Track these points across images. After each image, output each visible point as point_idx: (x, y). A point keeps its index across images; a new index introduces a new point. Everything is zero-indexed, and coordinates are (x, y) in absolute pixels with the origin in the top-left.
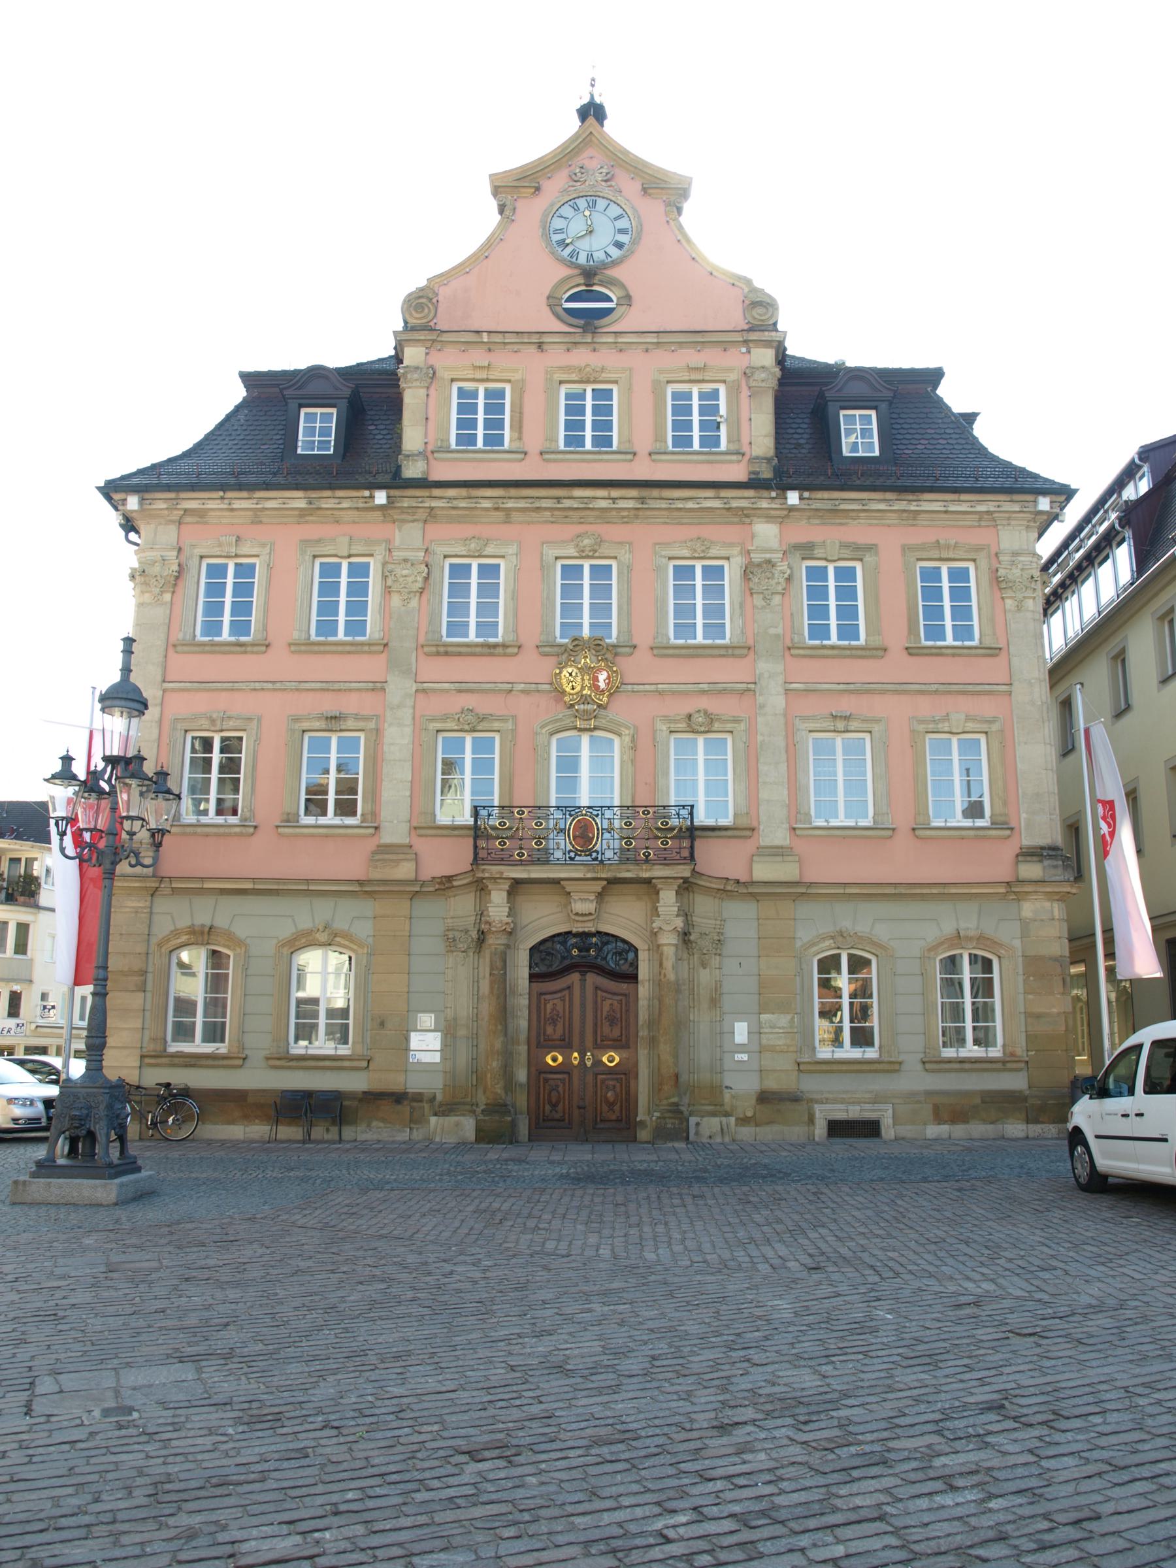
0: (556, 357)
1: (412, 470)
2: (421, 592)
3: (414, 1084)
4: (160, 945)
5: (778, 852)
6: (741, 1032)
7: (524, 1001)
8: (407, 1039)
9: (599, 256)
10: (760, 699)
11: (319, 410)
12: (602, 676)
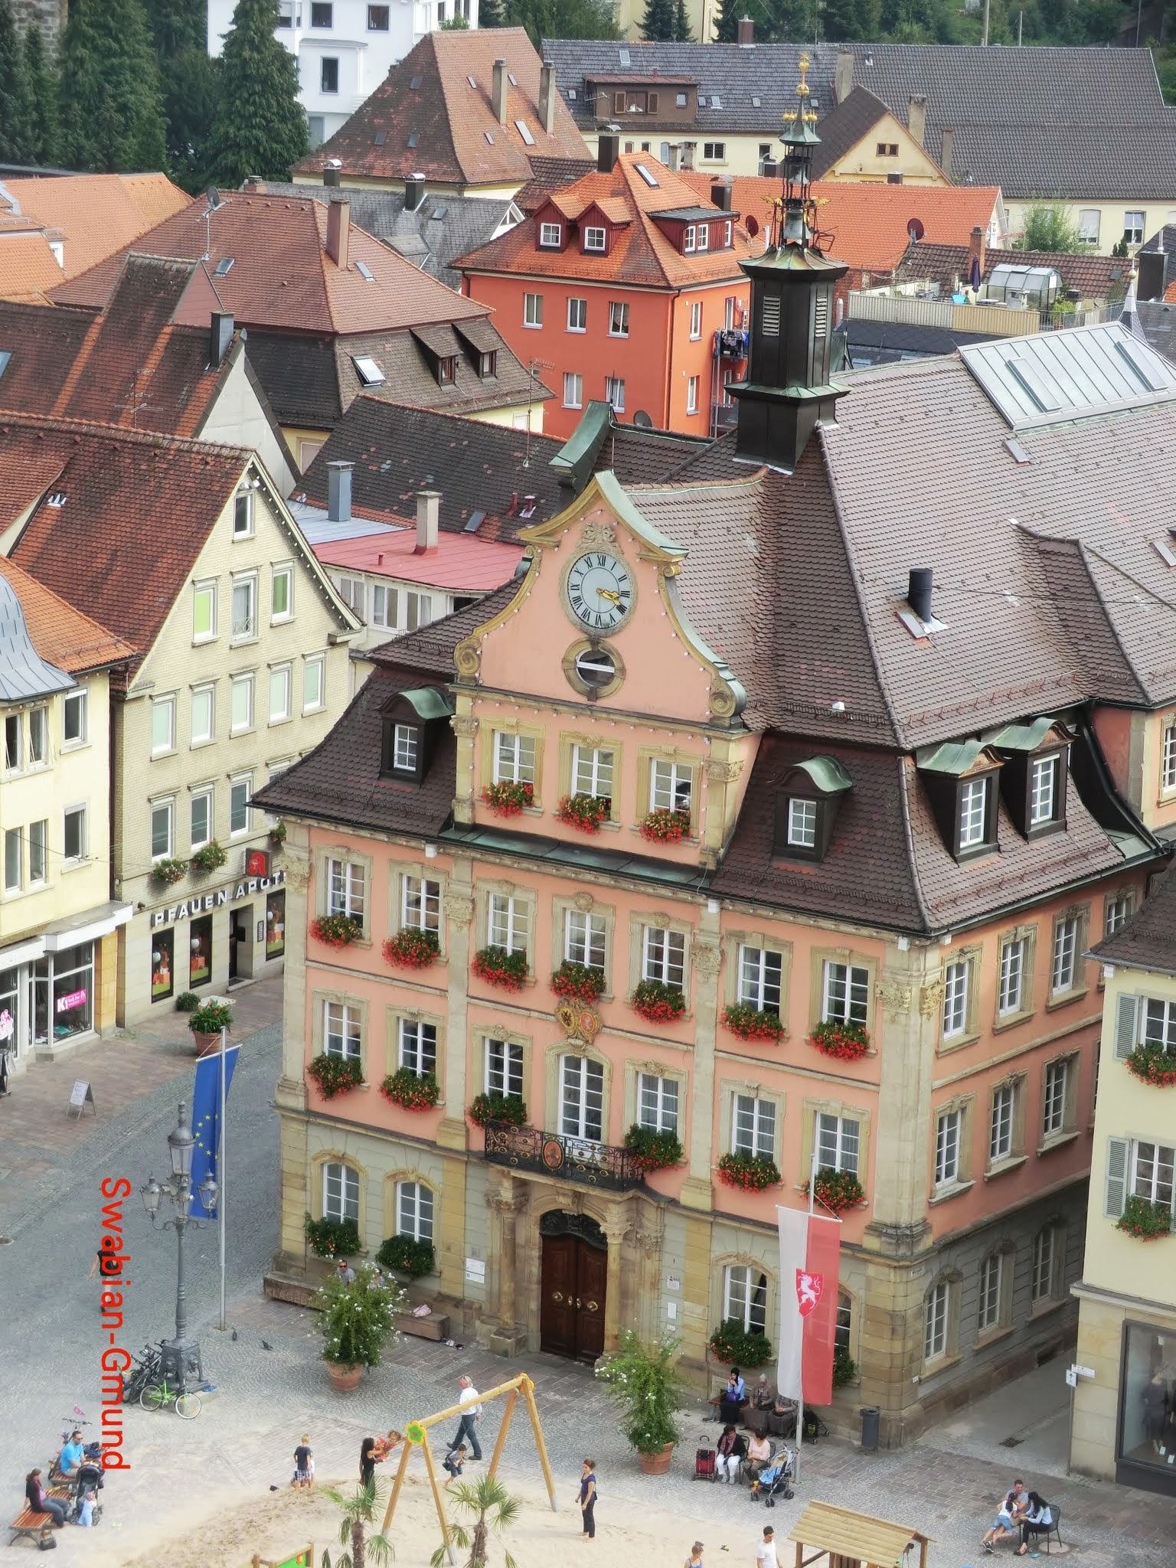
0: (570, 723)
1: (462, 816)
2: (470, 922)
3: (470, 1294)
4: (315, 1159)
5: (697, 1184)
6: (671, 1310)
7: (536, 1253)
8: (464, 1263)
9: (605, 618)
10: (697, 1060)
11: (397, 739)
12: (587, 1021)
